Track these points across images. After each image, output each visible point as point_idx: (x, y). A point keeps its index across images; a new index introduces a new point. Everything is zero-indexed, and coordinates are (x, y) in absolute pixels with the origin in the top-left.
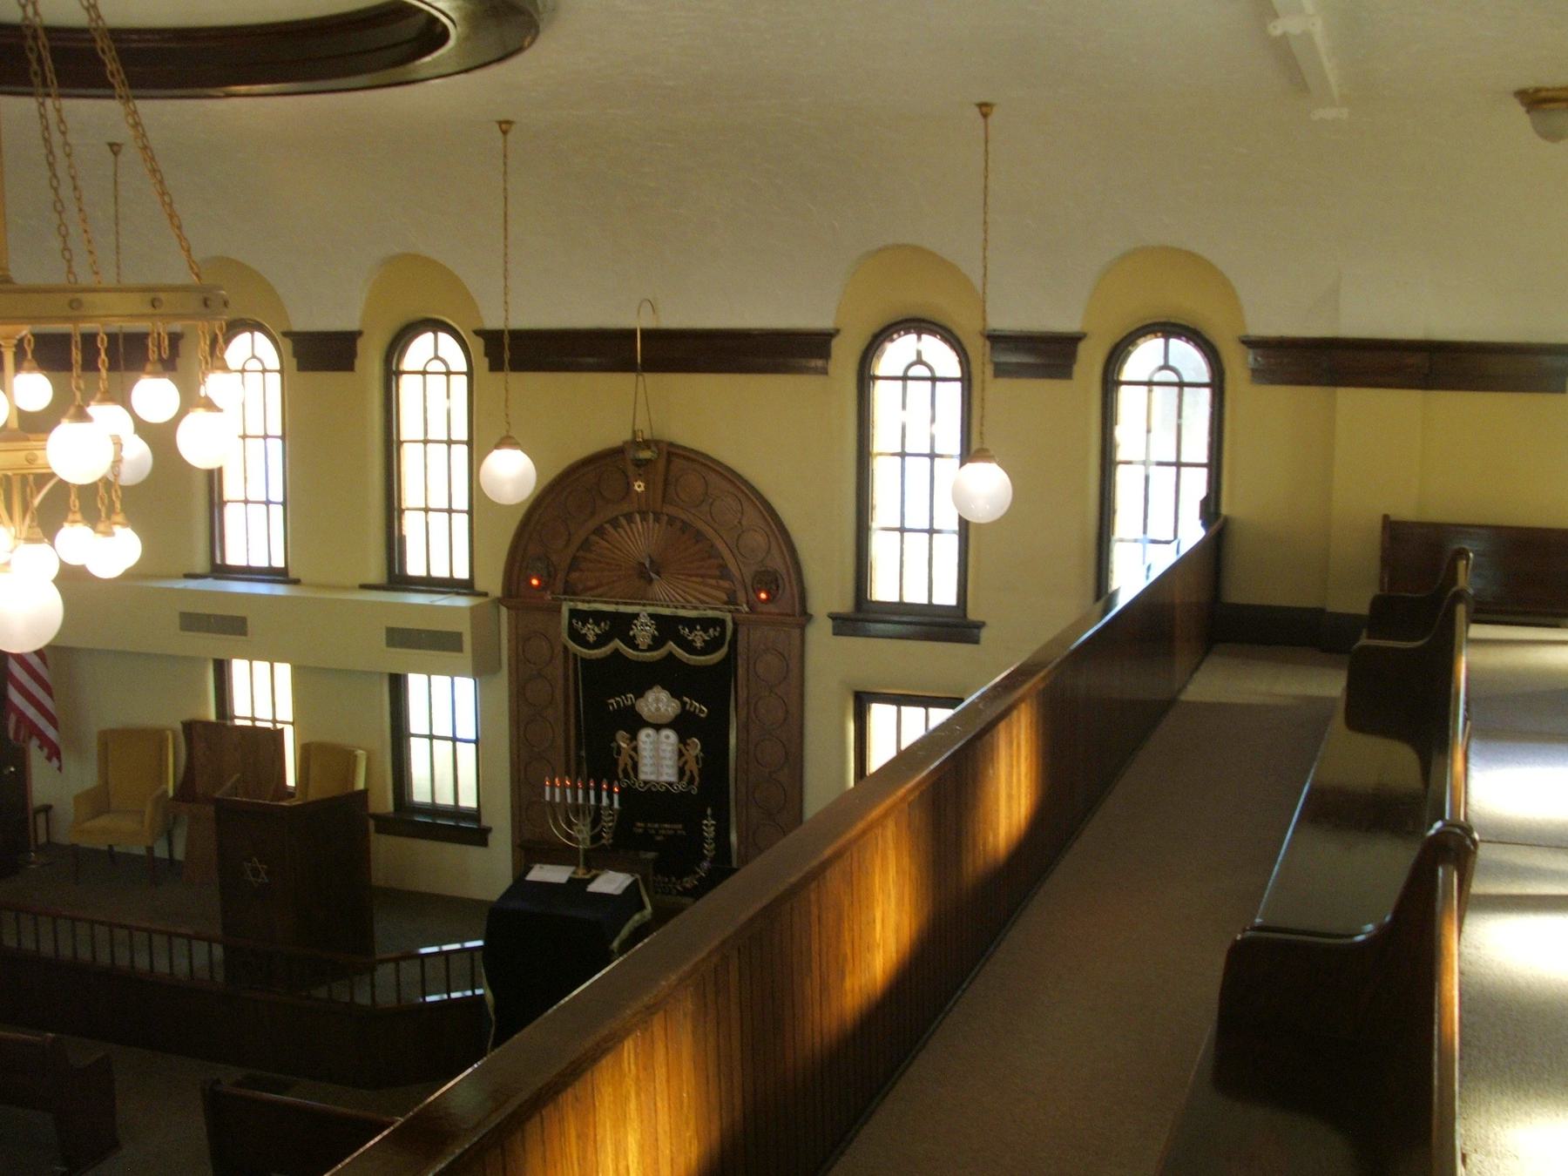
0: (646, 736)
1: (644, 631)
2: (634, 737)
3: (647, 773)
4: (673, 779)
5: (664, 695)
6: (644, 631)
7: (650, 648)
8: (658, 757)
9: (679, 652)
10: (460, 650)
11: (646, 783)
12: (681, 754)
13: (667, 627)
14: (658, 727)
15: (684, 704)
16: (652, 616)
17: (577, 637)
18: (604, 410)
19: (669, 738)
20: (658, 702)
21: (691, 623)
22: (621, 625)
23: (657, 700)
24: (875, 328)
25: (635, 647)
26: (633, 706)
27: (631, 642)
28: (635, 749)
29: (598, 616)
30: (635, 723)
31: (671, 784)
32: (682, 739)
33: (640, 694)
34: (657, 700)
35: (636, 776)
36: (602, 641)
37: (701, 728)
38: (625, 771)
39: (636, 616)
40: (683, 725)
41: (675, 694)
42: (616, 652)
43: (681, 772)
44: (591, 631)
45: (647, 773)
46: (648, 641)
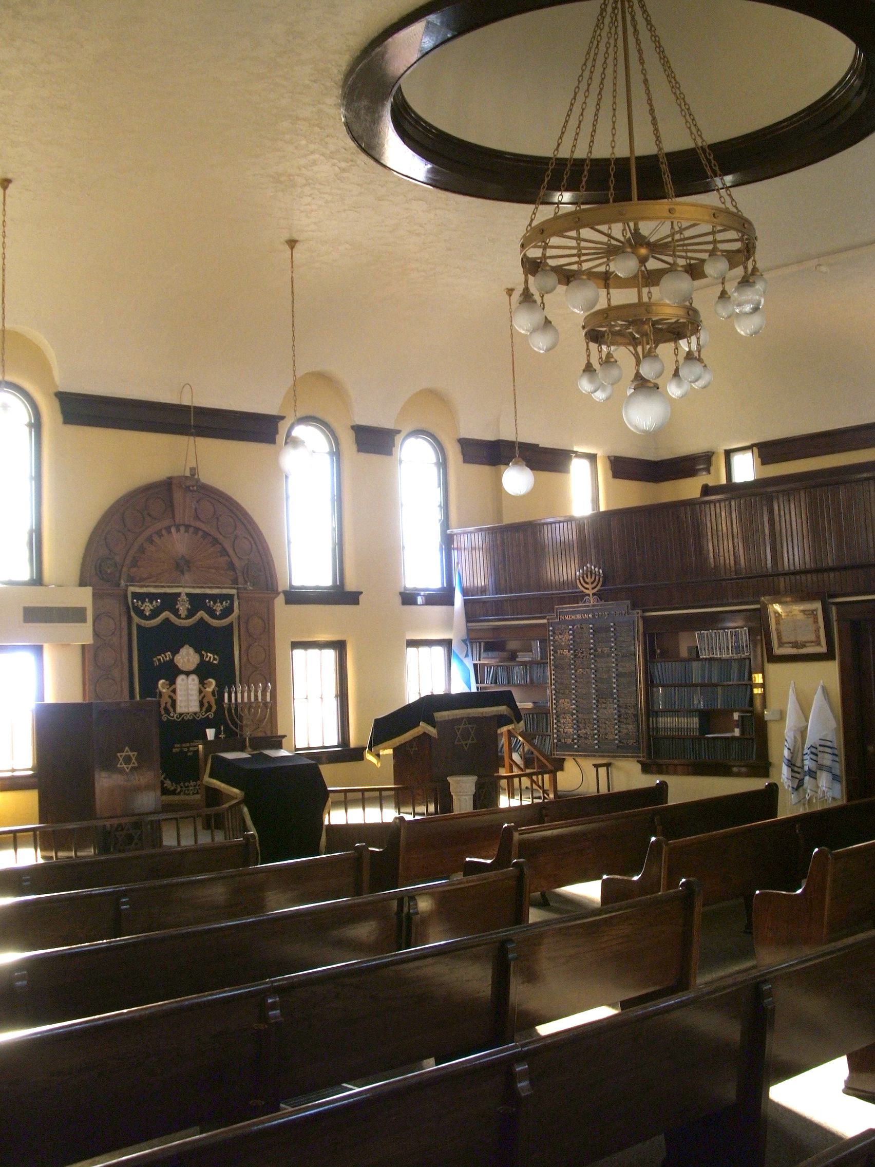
0: (180, 679)
1: (183, 607)
2: (172, 682)
3: (181, 707)
4: (197, 709)
5: (191, 651)
6: (183, 607)
7: (187, 617)
8: (188, 695)
9: (206, 617)
10: (83, 620)
11: (181, 714)
12: (200, 692)
13: (197, 602)
14: (188, 674)
15: (202, 656)
16: (188, 595)
17: (141, 614)
18: (152, 456)
19: (194, 680)
20: (187, 657)
21: (214, 598)
22: (169, 602)
23: (188, 654)
24: (318, 415)
25: (179, 617)
26: (172, 660)
27: (176, 613)
28: (174, 691)
29: (152, 597)
30: (172, 672)
31: (195, 714)
32: (202, 682)
33: (175, 652)
34: (188, 654)
35: (175, 711)
36: (155, 613)
37: (218, 672)
38: (166, 709)
39: (179, 594)
40: (203, 672)
41: (197, 650)
42: (167, 619)
43: (201, 704)
44: (147, 607)
45: (181, 707)
46: (186, 613)
